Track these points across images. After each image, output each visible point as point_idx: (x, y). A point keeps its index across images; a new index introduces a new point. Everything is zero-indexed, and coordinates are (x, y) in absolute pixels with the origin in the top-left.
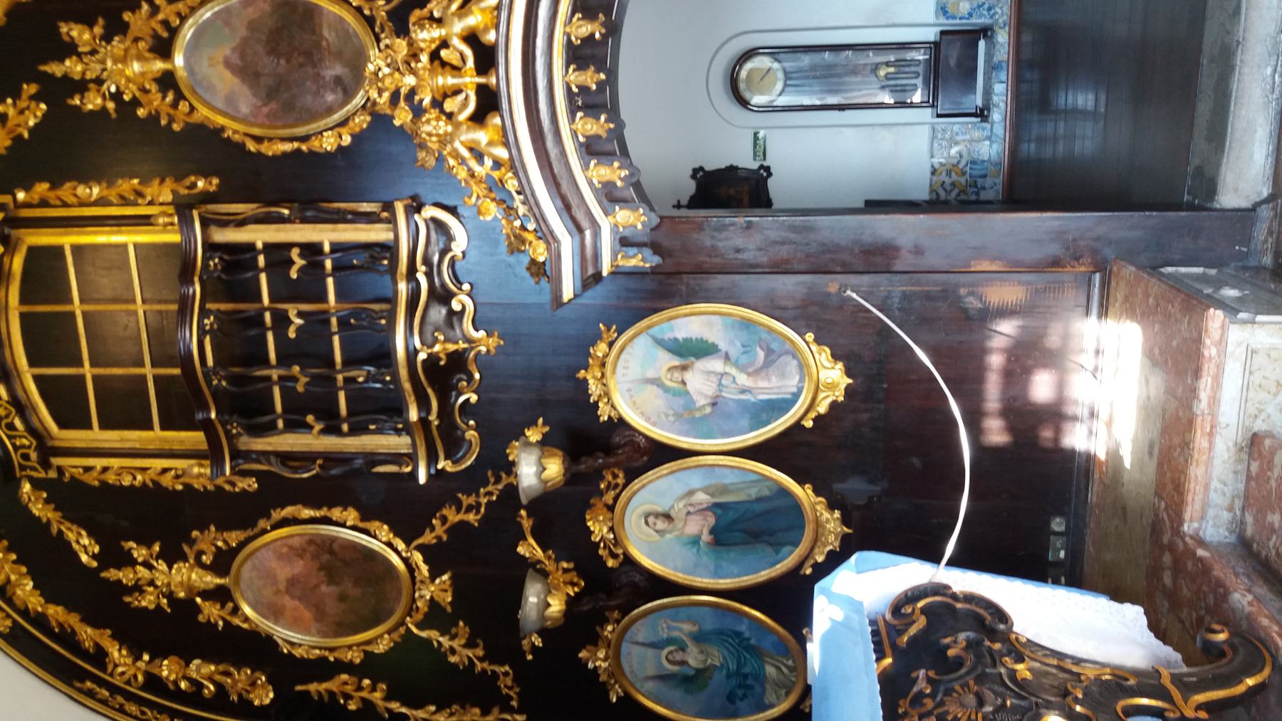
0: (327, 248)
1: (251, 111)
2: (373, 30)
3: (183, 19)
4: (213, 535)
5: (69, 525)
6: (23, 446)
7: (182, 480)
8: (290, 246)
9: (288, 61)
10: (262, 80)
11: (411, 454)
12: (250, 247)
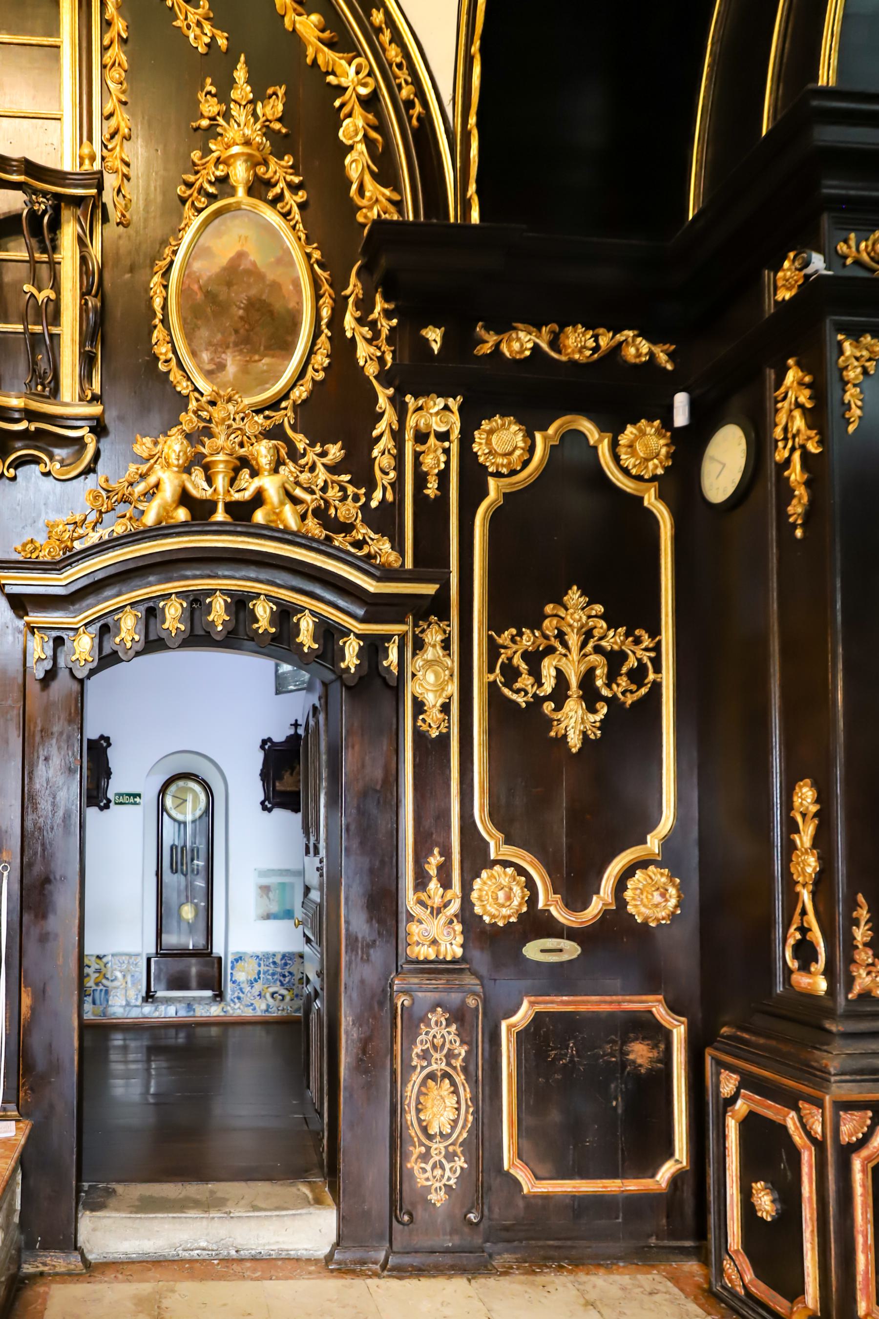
1: (195, 272)
2: (268, 408)
3: (286, 215)
9: (241, 318)
12: (55, 248)
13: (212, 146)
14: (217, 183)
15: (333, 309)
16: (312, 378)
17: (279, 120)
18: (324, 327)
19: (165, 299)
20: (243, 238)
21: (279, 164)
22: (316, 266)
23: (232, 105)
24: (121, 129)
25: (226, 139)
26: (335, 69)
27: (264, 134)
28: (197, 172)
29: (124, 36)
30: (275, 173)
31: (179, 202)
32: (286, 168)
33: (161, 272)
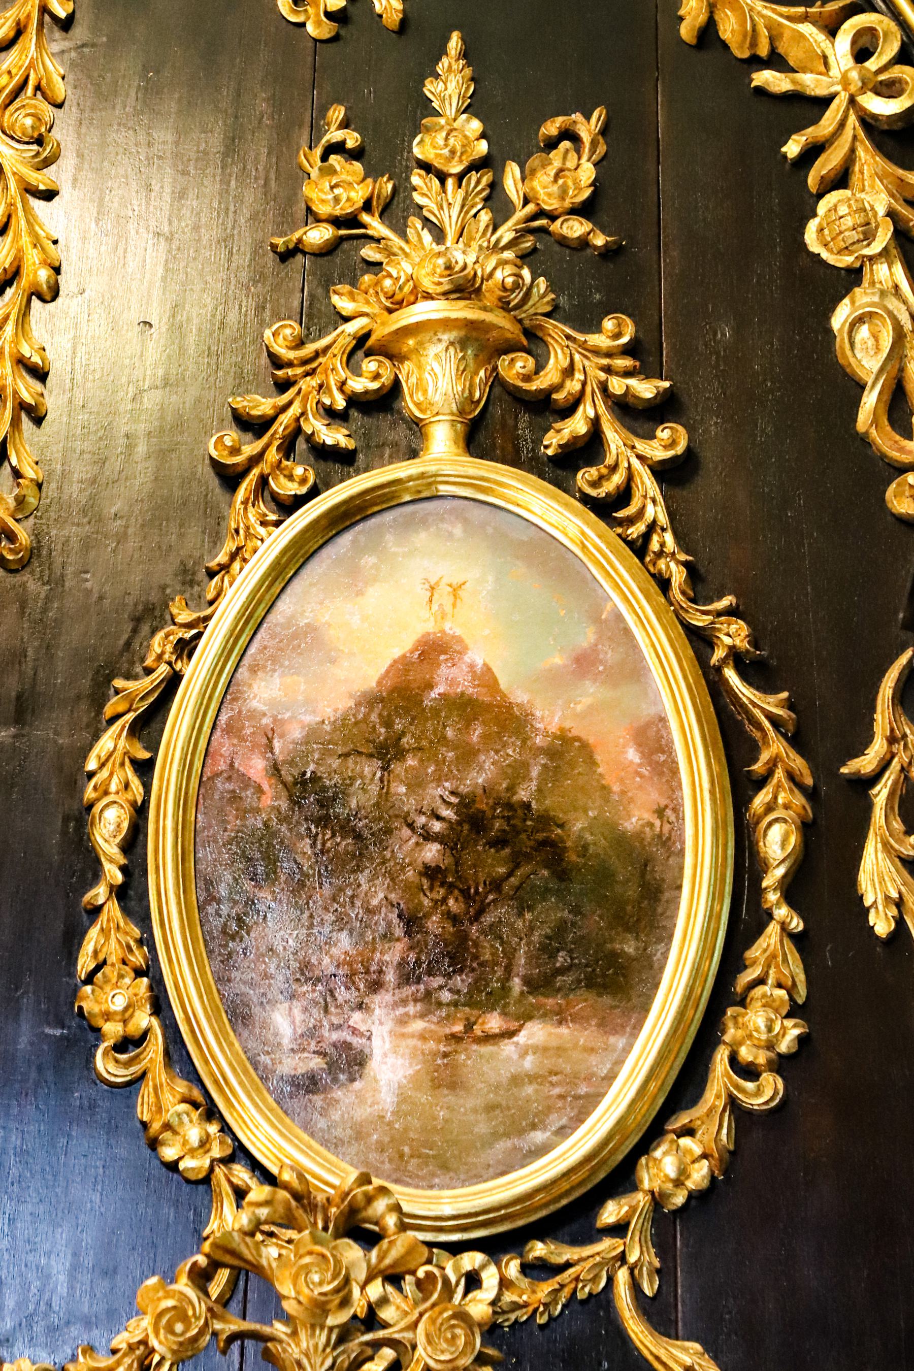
1: (254, 715)
9: (431, 873)
10: (370, 768)
13: (343, 304)
14: (354, 414)
15: (807, 828)
16: (733, 1103)
17: (584, 210)
18: (773, 897)
19: (140, 811)
20: (443, 590)
21: (583, 345)
22: (731, 675)
23: (416, 180)
24: (24, 272)
25: (388, 283)
26: (781, 50)
27: (525, 258)
28: (283, 386)
30: (569, 372)
31: (214, 482)
32: (609, 355)
33: (130, 717)
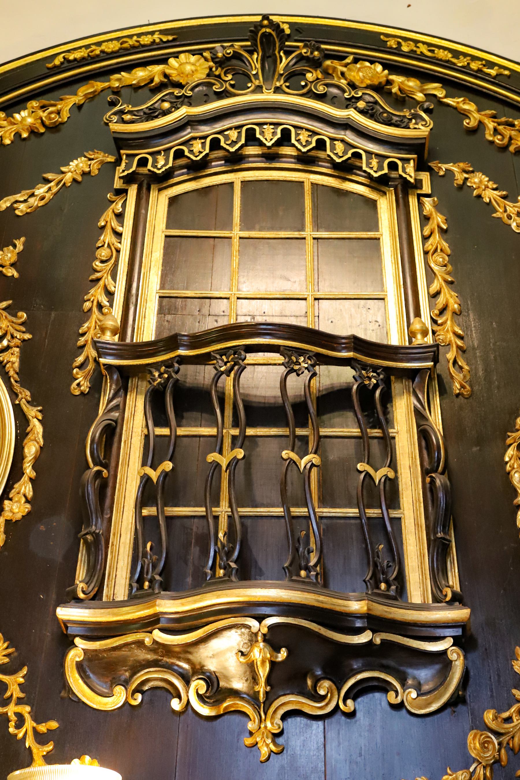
0: (394, 514)
4: (18, 335)
5: (55, 190)
6: (155, 161)
7: (95, 309)
8: (393, 465)
11: (101, 599)
24: (450, 305)
29: (445, 227)
